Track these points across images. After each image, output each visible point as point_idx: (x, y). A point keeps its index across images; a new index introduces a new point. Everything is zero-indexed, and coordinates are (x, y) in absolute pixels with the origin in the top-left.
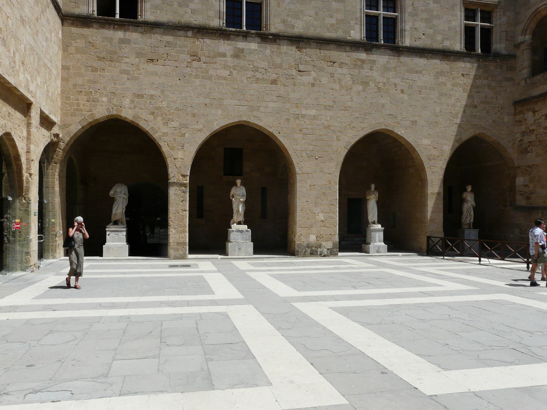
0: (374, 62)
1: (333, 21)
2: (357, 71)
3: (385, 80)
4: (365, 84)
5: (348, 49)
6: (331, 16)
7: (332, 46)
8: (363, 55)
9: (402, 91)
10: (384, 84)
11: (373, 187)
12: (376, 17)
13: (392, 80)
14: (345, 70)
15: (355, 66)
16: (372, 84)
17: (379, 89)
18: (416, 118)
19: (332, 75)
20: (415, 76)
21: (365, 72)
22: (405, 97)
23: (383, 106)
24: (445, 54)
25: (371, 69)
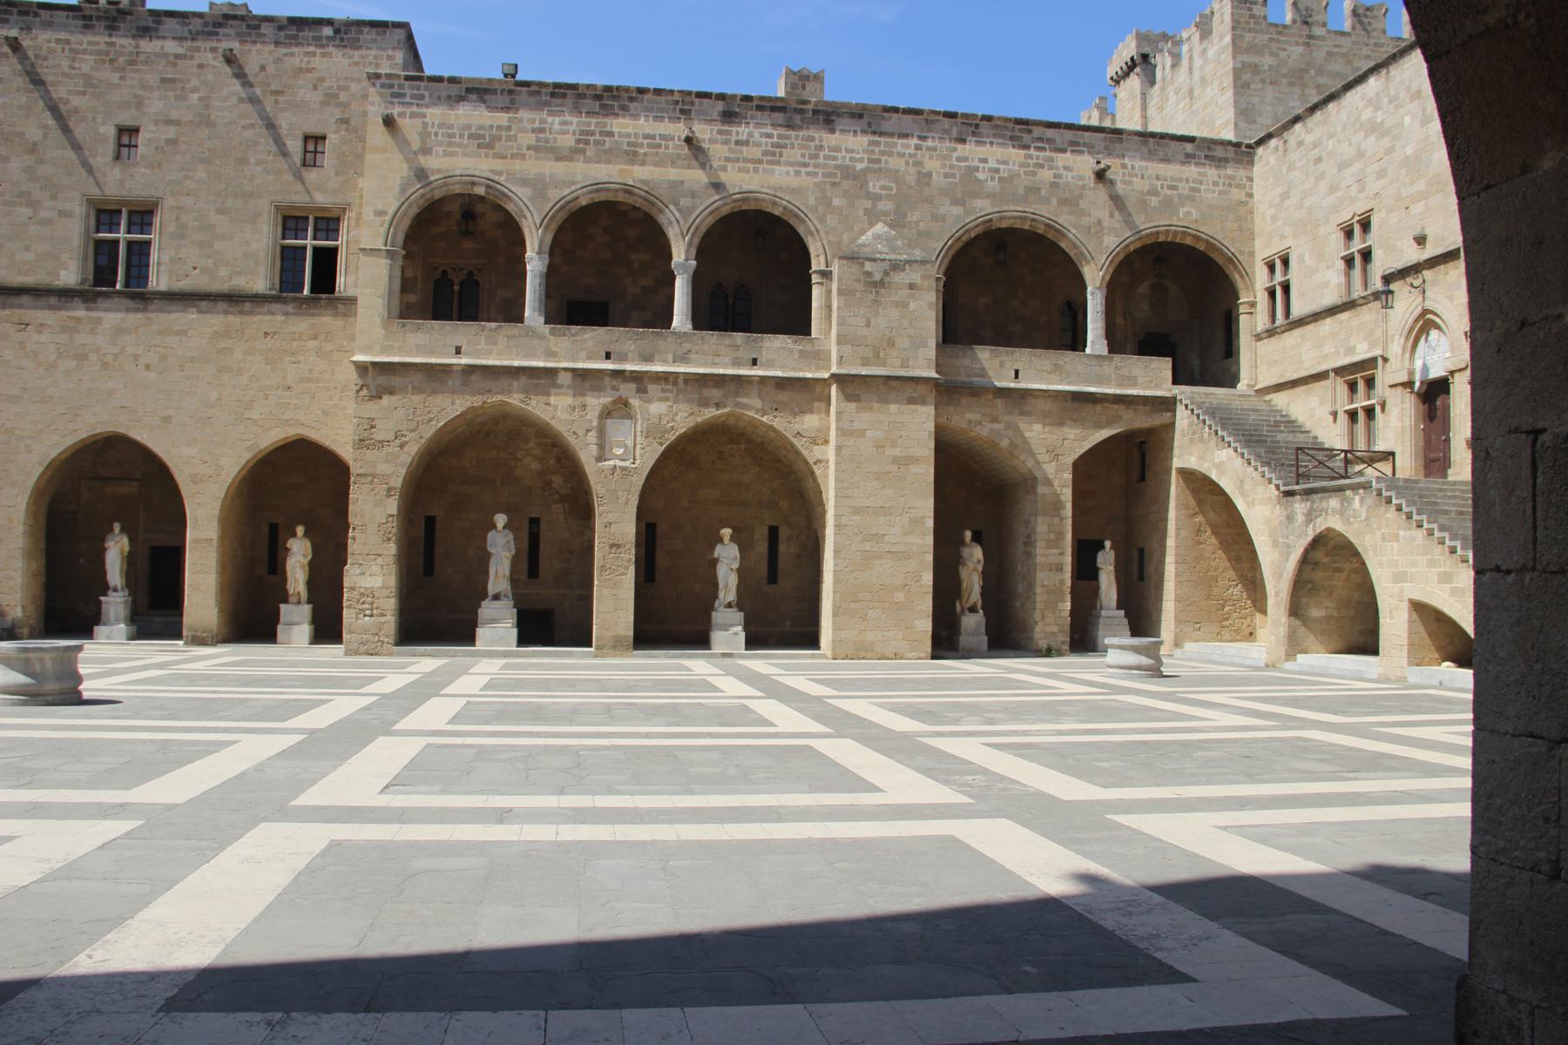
0: (99, 320)
1: (30, 256)
2: (66, 337)
3: (116, 350)
4: (82, 357)
5: (53, 300)
6: (27, 249)
7: (25, 299)
8: (81, 313)
9: (148, 367)
10: (116, 356)
11: (117, 527)
12: (116, 242)
13: (131, 350)
14: (45, 337)
15: (64, 329)
16: (93, 358)
17: (105, 365)
18: (170, 412)
19: (22, 345)
20: (172, 341)
21: (82, 338)
22: (152, 375)
23: (111, 393)
24: (234, 300)
25: (93, 332)
